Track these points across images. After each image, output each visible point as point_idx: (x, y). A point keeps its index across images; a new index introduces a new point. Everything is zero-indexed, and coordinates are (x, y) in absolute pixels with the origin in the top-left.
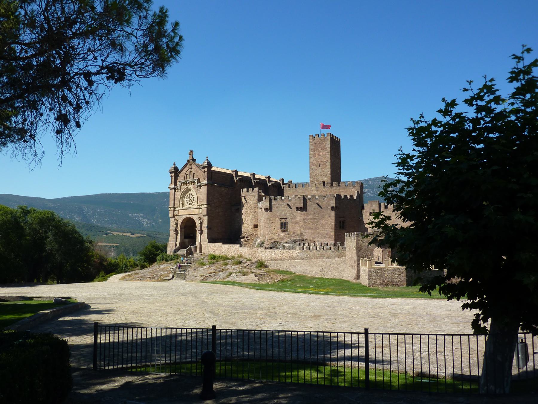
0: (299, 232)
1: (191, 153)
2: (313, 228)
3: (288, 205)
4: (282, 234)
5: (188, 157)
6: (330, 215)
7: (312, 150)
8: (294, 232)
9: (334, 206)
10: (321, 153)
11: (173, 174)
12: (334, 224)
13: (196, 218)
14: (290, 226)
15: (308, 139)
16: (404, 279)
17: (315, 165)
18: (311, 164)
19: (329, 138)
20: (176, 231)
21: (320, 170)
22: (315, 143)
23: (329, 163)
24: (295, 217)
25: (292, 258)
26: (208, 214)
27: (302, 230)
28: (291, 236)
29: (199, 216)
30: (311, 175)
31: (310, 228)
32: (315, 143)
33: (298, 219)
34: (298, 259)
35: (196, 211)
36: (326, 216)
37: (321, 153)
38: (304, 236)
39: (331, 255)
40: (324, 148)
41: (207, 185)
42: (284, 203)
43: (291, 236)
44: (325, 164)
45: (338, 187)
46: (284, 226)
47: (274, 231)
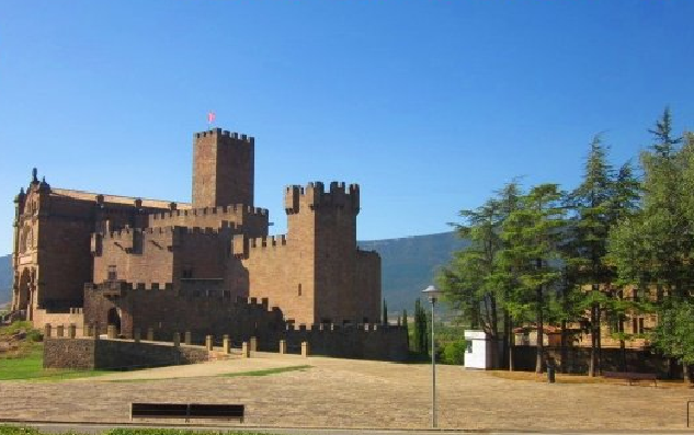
1: (35, 171)
3: (116, 243)
5: (31, 179)
7: (196, 159)
9: (171, 244)
11: (17, 205)
12: (171, 274)
13: (29, 266)
15: (191, 140)
16: (92, 357)
17: (199, 181)
18: (195, 180)
19: (215, 136)
20: (16, 287)
23: (214, 178)
24: (125, 263)
26: (39, 262)
40: (209, 155)
41: (39, 217)
42: (112, 242)
45: (214, 216)
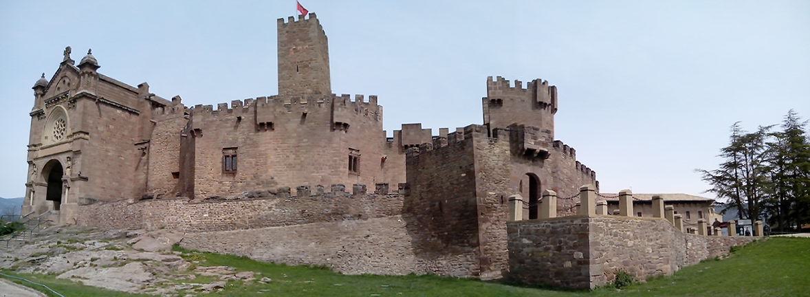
0: (264, 177)
2: (299, 167)
4: (227, 181)
6: (330, 140)
8: (255, 176)
10: (301, 47)
14: (245, 165)
18: (281, 68)
21: (299, 76)
22: (287, 32)
24: (255, 145)
25: (259, 223)
27: (271, 172)
28: (248, 185)
29: (69, 155)
30: (281, 87)
31: (290, 166)
32: (287, 32)
33: (262, 148)
34: (274, 223)
35: (67, 147)
36: (323, 144)
37: (299, 48)
38: (277, 184)
39: (368, 210)
43: (248, 185)
44: (307, 66)
46: (230, 166)
47: (210, 177)
